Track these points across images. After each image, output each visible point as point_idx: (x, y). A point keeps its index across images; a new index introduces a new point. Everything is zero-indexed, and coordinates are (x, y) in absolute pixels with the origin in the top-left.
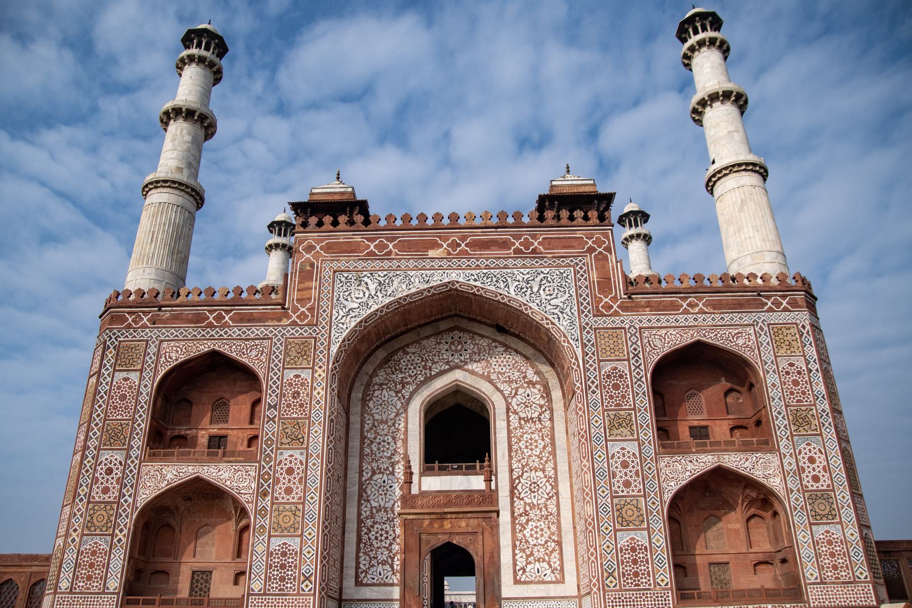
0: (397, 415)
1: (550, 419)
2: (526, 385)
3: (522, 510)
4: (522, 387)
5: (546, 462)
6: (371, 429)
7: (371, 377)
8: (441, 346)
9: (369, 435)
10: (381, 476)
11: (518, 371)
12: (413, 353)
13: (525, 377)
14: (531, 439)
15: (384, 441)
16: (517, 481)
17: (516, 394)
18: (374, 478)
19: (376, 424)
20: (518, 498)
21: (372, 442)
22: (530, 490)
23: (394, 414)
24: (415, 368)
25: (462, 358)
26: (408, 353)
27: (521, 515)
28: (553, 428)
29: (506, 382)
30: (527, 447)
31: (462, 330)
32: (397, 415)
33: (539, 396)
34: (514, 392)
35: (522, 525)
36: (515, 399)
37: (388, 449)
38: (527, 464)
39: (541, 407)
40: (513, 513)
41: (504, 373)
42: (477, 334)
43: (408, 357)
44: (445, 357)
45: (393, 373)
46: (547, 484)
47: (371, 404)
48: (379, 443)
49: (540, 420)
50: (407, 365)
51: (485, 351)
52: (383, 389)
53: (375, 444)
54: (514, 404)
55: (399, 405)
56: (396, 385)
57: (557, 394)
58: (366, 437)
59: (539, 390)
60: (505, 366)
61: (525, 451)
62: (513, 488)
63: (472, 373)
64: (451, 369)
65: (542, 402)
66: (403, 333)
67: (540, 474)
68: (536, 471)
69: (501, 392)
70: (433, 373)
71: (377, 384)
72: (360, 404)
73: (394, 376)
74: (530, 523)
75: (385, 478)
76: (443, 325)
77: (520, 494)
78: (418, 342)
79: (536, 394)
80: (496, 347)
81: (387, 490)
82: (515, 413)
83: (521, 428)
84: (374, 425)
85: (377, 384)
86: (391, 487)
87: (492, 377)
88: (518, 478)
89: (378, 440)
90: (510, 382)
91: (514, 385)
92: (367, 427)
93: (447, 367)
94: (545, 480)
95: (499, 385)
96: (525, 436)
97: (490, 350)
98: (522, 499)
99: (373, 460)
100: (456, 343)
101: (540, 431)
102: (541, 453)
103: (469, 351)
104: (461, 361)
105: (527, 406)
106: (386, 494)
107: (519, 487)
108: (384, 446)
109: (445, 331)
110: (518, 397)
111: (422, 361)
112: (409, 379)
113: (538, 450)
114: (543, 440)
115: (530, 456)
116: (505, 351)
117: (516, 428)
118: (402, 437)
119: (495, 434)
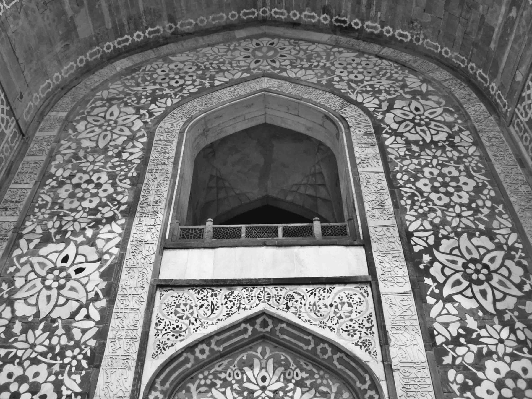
0: (132, 139)
1: (474, 144)
2: (408, 96)
3: (454, 329)
4: (403, 99)
5: (492, 215)
6: (69, 161)
7: (95, 90)
8: (237, 53)
9: (60, 172)
10: (63, 245)
11: (389, 79)
12: (182, 62)
13: (404, 86)
14: (441, 175)
15: (89, 182)
16: (426, 258)
17: (390, 108)
18: (43, 251)
19: (81, 154)
20: (439, 297)
21: (61, 184)
22: (467, 277)
23: (126, 138)
24: (181, 78)
25: (277, 65)
26: (172, 62)
27: (455, 341)
28: (485, 158)
29: (367, 92)
30: (435, 190)
31: (273, 37)
32: (132, 139)
33: (439, 111)
34: (385, 106)
35: (462, 369)
36: (389, 117)
37: (96, 195)
38: (444, 223)
39: (450, 125)
40: (429, 336)
41: (362, 81)
42: (302, 40)
43: (172, 66)
44: (242, 63)
45: (138, 85)
46: (508, 263)
47: (81, 126)
48: (78, 185)
49: (453, 146)
50: (167, 75)
51: (319, 55)
52: (111, 105)
53: (68, 187)
54: (389, 118)
55: (139, 124)
56: (139, 99)
57: (476, 109)
58: (51, 176)
59: (439, 103)
60: (359, 73)
61: (434, 196)
62: (418, 274)
63: (295, 81)
64: (253, 77)
65: (450, 119)
66: (166, 41)
67: (484, 241)
68: (471, 236)
69: (360, 105)
70: (217, 83)
71: (102, 99)
72: (58, 126)
73: (140, 89)
74: (490, 365)
75: (71, 250)
76: (240, 33)
77: (441, 286)
78: (195, 49)
79: (434, 108)
80: (340, 52)
81: (68, 278)
82: (394, 133)
83: (412, 157)
84: (76, 156)
85: (102, 99)
86: (79, 271)
87: (337, 86)
88: (428, 250)
89: (75, 181)
90: (375, 93)
91: (383, 96)
92: (59, 159)
93: (245, 75)
94: (500, 255)
95: (353, 96)
96: (427, 170)
97: (328, 55)
98: (450, 299)
99: (52, 215)
100: (264, 50)
101: (459, 160)
102: (472, 200)
103: (289, 57)
104: (274, 68)
105: (419, 125)
106: (61, 287)
107: (435, 271)
108: (86, 190)
109: (244, 39)
110: (398, 112)
111: (199, 68)
112: (168, 91)
113: (462, 194)
114: (471, 177)
115: (447, 206)
116: (356, 56)
117: (403, 158)
118: (133, 173)
119: (354, 165)
